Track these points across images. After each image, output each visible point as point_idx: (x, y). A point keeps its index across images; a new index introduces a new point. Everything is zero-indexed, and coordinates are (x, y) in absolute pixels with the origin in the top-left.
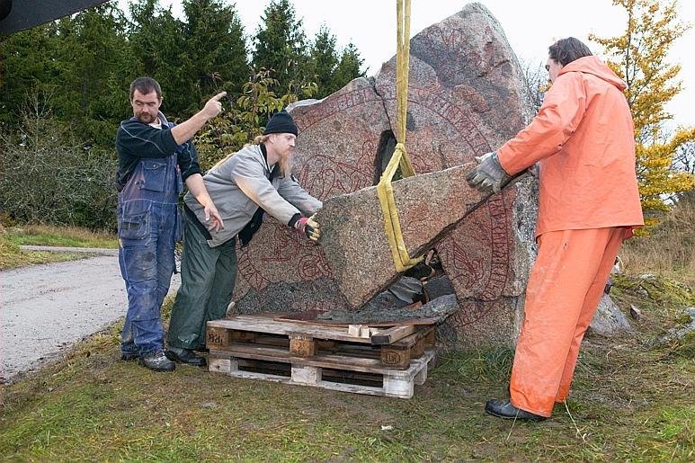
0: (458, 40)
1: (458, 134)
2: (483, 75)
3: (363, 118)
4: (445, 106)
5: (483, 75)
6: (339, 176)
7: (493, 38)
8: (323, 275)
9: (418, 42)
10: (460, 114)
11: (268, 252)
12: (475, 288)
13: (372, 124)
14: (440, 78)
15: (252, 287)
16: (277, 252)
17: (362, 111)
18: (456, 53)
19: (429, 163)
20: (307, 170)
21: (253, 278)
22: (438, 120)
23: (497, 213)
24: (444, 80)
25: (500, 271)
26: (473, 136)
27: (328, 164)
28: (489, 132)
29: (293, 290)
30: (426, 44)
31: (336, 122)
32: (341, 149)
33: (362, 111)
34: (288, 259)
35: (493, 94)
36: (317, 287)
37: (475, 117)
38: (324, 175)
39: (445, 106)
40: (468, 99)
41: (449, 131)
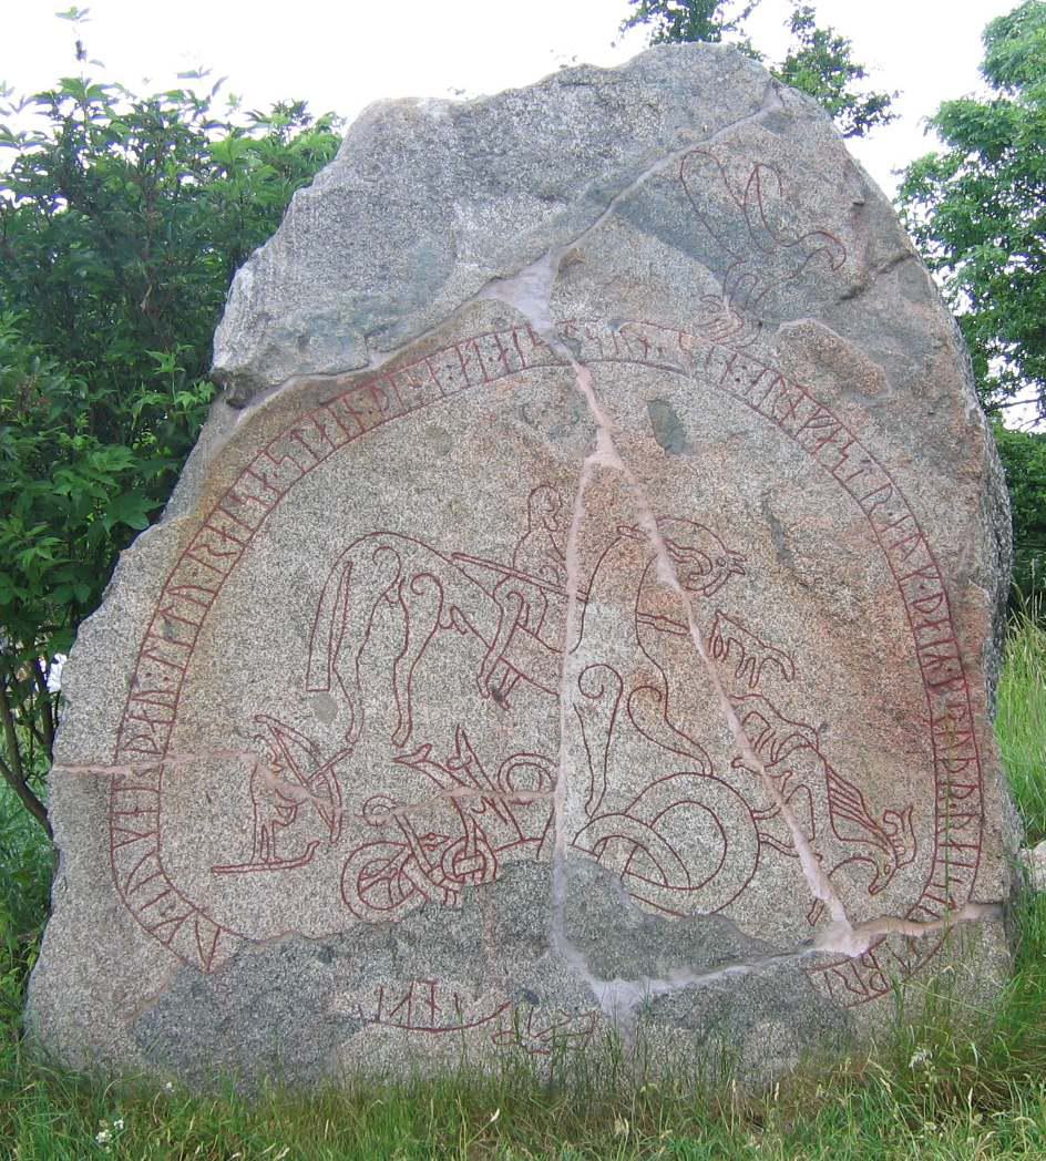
0: (772, 191)
1: (808, 462)
2: (855, 293)
3: (524, 418)
4: (765, 381)
5: (855, 293)
6: (456, 595)
7: (866, 192)
8: (428, 900)
9: (656, 194)
10: (806, 406)
11: (234, 843)
12: (896, 889)
13: (552, 436)
14: (732, 295)
15: (184, 960)
16: (265, 841)
17: (515, 396)
18: (770, 229)
19: (738, 545)
20: (348, 580)
21: (186, 931)
22: (750, 421)
23: (941, 677)
24: (746, 305)
25: (960, 836)
26: (852, 465)
27: (418, 560)
28: (895, 454)
29: (328, 955)
30: (681, 200)
31: (434, 432)
32: (456, 514)
33: (515, 396)
34: (300, 862)
35: (891, 346)
36: (411, 939)
37: (850, 409)
38: (405, 593)
39: (765, 381)
40: (825, 359)
41: (784, 451)
